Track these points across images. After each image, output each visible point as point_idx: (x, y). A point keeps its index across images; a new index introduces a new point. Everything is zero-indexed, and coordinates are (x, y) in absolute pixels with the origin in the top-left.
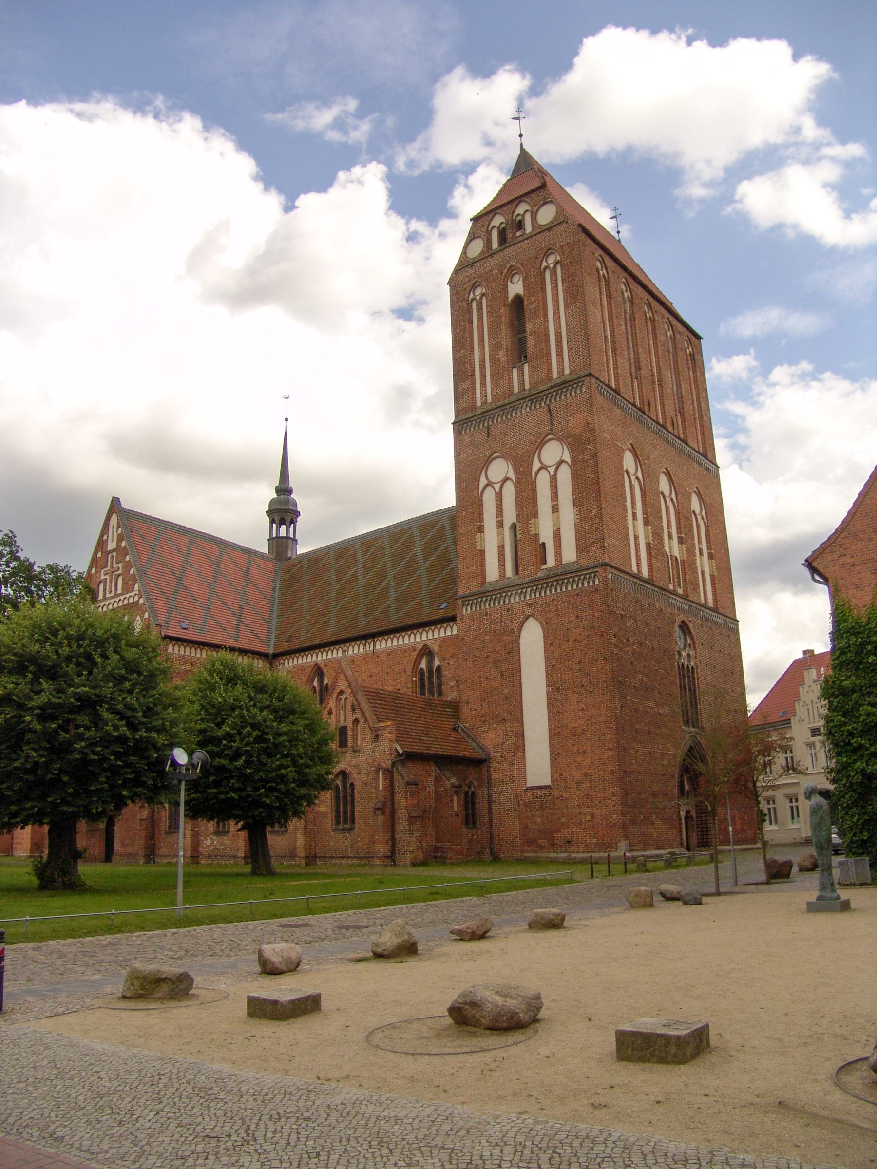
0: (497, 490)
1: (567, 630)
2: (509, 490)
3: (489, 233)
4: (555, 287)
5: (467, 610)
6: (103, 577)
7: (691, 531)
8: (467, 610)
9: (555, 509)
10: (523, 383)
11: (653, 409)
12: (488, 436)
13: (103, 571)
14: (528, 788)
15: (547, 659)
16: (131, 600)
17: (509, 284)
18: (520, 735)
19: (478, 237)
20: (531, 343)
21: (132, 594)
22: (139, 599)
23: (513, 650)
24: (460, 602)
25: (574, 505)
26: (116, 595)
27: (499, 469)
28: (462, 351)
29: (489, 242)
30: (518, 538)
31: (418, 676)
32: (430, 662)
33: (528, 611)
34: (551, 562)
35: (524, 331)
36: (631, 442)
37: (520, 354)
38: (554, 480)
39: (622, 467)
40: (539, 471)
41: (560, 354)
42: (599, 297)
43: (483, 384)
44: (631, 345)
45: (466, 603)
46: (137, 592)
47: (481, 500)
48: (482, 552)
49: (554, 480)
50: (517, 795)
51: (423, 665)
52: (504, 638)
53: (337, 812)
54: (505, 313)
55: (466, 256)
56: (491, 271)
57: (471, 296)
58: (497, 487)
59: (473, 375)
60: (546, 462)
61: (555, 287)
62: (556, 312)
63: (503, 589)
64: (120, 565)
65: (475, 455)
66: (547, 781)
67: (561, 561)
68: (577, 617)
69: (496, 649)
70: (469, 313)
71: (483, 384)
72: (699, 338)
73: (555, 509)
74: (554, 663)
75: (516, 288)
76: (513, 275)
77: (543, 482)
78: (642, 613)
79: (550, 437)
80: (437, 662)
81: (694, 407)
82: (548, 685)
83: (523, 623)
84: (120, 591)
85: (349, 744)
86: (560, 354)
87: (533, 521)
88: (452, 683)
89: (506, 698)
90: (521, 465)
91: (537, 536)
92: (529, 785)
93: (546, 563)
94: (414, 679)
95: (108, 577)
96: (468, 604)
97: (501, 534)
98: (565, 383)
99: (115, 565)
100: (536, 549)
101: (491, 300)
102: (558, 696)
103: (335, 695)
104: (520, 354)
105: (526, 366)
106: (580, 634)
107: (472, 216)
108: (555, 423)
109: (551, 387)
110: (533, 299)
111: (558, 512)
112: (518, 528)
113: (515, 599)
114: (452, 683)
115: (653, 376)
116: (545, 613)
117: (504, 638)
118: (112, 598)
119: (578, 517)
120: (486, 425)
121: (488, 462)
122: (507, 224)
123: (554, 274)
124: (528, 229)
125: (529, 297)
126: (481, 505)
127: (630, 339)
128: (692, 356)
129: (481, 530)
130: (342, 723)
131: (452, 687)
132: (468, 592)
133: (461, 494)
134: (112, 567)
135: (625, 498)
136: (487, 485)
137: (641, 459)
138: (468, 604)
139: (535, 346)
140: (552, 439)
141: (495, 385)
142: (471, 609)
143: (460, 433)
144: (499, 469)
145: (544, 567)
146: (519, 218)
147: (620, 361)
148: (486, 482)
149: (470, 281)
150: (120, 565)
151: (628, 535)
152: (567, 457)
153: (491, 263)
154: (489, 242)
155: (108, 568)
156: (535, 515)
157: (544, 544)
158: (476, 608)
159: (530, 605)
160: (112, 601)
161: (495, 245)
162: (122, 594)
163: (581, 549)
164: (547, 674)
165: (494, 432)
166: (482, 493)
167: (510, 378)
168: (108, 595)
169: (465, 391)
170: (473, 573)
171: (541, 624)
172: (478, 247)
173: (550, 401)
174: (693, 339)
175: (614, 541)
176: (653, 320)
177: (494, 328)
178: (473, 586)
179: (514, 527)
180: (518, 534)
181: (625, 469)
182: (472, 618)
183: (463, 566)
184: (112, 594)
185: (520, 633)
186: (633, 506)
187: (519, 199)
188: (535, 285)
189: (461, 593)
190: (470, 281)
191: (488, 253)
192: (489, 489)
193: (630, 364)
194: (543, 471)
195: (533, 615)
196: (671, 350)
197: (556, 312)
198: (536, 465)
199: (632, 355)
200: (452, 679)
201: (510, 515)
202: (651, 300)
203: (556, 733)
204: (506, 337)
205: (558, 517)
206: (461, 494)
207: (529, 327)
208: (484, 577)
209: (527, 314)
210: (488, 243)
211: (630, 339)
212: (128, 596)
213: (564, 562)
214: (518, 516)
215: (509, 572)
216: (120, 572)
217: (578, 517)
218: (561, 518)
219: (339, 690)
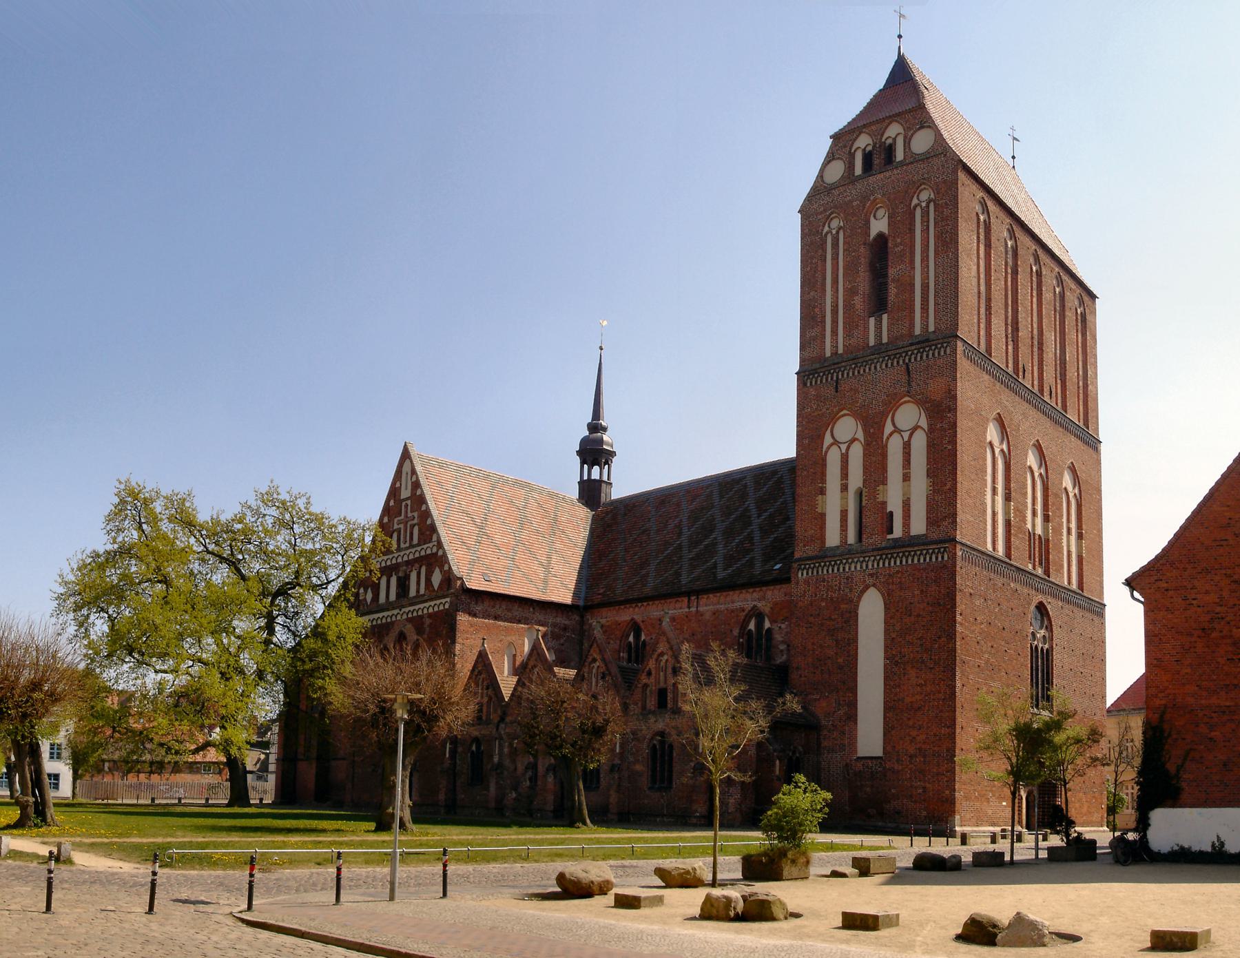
0: (844, 451)
1: (911, 603)
2: (857, 452)
3: (852, 156)
4: (926, 230)
5: (802, 575)
6: (396, 527)
7: (1060, 509)
8: (802, 575)
9: (906, 478)
10: (881, 337)
11: (1028, 375)
12: (837, 392)
13: (396, 520)
14: (858, 758)
15: (887, 631)
16: (429, 552)
17: (872, 218)
18: (853, 705)
19: (838, 158)
20: (892, 290)
21: (430, 545)
22: (438, 550)
23: (851, 618)
24: (795, 565)
25: (928, 476)
26: (412, 546)
27: (847, 428)
28: (812, 294)
29: (850, 166)
30: (864, 504)
31: (746, 637)
32: (760, 625)
33: (870, 581)
34: (898, 532)
35: (886, 276)
36: (999, 411)
37: (879, 304)
38: (907, 446)
39: (986, 439)
40: (891, 434)
41: (925, 308)
42: (975, 248)
43: (835, 332)
44: (1010, 303)
45: (803, 566)
46: (436, 543)
47: (824, 460)
48: (823, 516)
49: (907, 446)
50: (847, 765)
51: (752, 626)
52: (842, 606)
53: (654, 770)
54: (864, 252)
55: (823, 181)
56: (851, 201)
57: (826, 229)
58: (844, 447)
59: (823, 322)
60: (900, 425)
61: (926, 230)
62: (925, 259)
63: (844, 553)
64: (416, 514)
65: (821, 410)
66: (879, 752)
67: (909, 532)
68: (922, 591)
69: (833, 617)
70: (823, 250)
71: (835, 332)
72: (1093, 297)
73: (906, 478)
74: (894, 636)
75: (879, 225)
76: (877, 209)
77: (895, 447)
78: (994, 592)
79: (907, 399)
80: (767, 625)
81: (1078, 375)
82: (886, 658)
83: (863, 592)
84: (415, 541)
85: (669, 706)
86: (925, 308)
87: (881, 487)
88: (782, 647)
89: (841, 667)
90: (872, 427)
91: (884, 503)
92: (861, 753)
93: (892, 533)
94: (741, 640)
95: (402, 526)
96: (805, 568)
97: (844, 499)
98: (927, 340)
99: (410, 515)
100: (882, 518)
101: (850, 236)
102: (895, 669)
103: (655, 656)
104: (879, 304)
105: (885, 317)
106: (924, 609)
107: (832, 133)
108: (913, 384)
109: (912, 344)
110: (899, 240)
111: (909, 480)
112: (864, 494)
113: (855, 568)
114: (782, 647)
115: (1032, 338)
116: (888, 584)
117: (842, 606)
118: (407, 548)
119: (931, 488)
120: (835, 378)
121: (834, 419)
122: (874, 146)
123: (925, 213)
124: (899, 155)
125: (894, 237)
126: (824, 465)
127: (1010, 296)
128: (1084, 316)
129: (822, 492)
130: (662, 685)
131: (782, 651)
132: (805, 555)
133: (802, 452)
134: (406, 516)
135: (986, 472)
136: (832, 445)
137: (1008, 430)
138: (805, 568)
139: (897, 295)
140: (909, 402)
141: (848, 334)
142: (807, 574)
143: (805, 384)
144: (847, 428)
145: (889, 537)
146: (889, 141)
147: (994, 320)
148: (831, 441)
149: (825, 211)
150: (416, 514)
151: (985, 511)
152: (924, 423)
153: (853, 192)
154: (850, 166)
155: (402, 517)
156: (884, 482)
157: (891, 514)
158: (812, 573)
159: (871, 575)
160: (408, 552)
161: (858, 170)
162: (418, 545)
163: (932, 521)
164: (886, 647)
165: (844, 386)
166: (826, 452)
167: (866, 328)
168: (402, 546)
169: (814, 339)
170: (812, 536)
171: (883, 595)
172: (837, 170)
173: (910, 360)
174: (1086, 298)
175: (968, 516)
176: (1039, 274)
177: (851, 268)
178: (811, 550)
179: (860, 494)
180: (864, 500)
181: (988, 440)
182: (807, 582)
183: (802, 528)
184: (407, 545)
185: (859, 602)
186: (994, 481)
187: (893, 118)
188: (902, 220)
189: (797, 555)
190: (825, 211)
191: (849, 178)
192: (834, 448)
193: (1006, 324)
194: (896, 435)
195: (874, 585)
196: (1058, 308)
197: (925, 259)
198: (889, 428)
199: (1010, 314)
200: (783, 642)
201: (856, 479)
202: (1040, 252)
203: (891, 706)
204: (863, 281)
205: (909, 486)
206: (802, 452)
207: (892, 272)
208: (822, 539)
209: (890, 257)
210: (849, 167)
211: (1010, 296)
212: (425, 546)
213: (912, 534)
214: (865, 481)
215: (851, 538)
216: (416, 521)
217: (931, 488)
218: (913, 489)
219: (659, 651)
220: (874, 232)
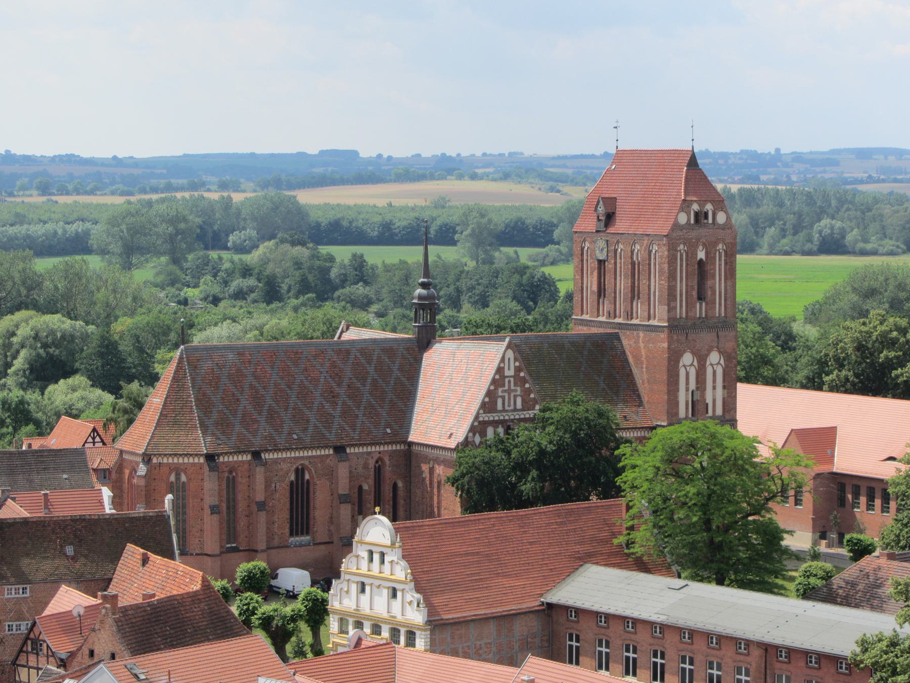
220: (698, 258)
